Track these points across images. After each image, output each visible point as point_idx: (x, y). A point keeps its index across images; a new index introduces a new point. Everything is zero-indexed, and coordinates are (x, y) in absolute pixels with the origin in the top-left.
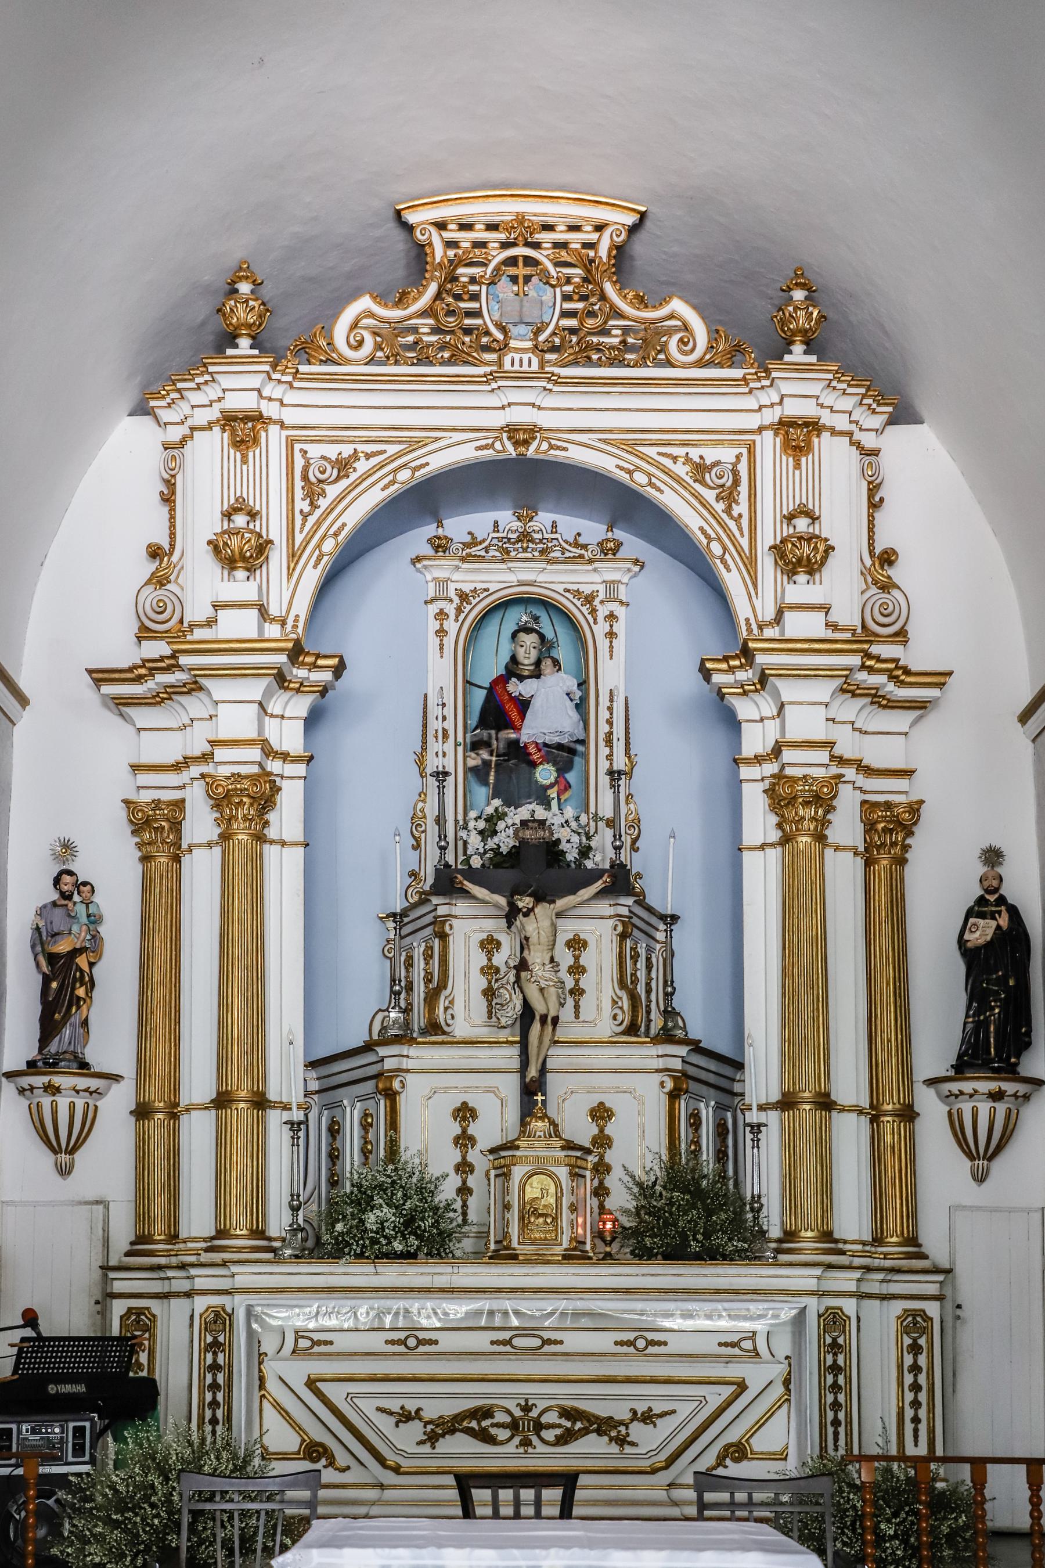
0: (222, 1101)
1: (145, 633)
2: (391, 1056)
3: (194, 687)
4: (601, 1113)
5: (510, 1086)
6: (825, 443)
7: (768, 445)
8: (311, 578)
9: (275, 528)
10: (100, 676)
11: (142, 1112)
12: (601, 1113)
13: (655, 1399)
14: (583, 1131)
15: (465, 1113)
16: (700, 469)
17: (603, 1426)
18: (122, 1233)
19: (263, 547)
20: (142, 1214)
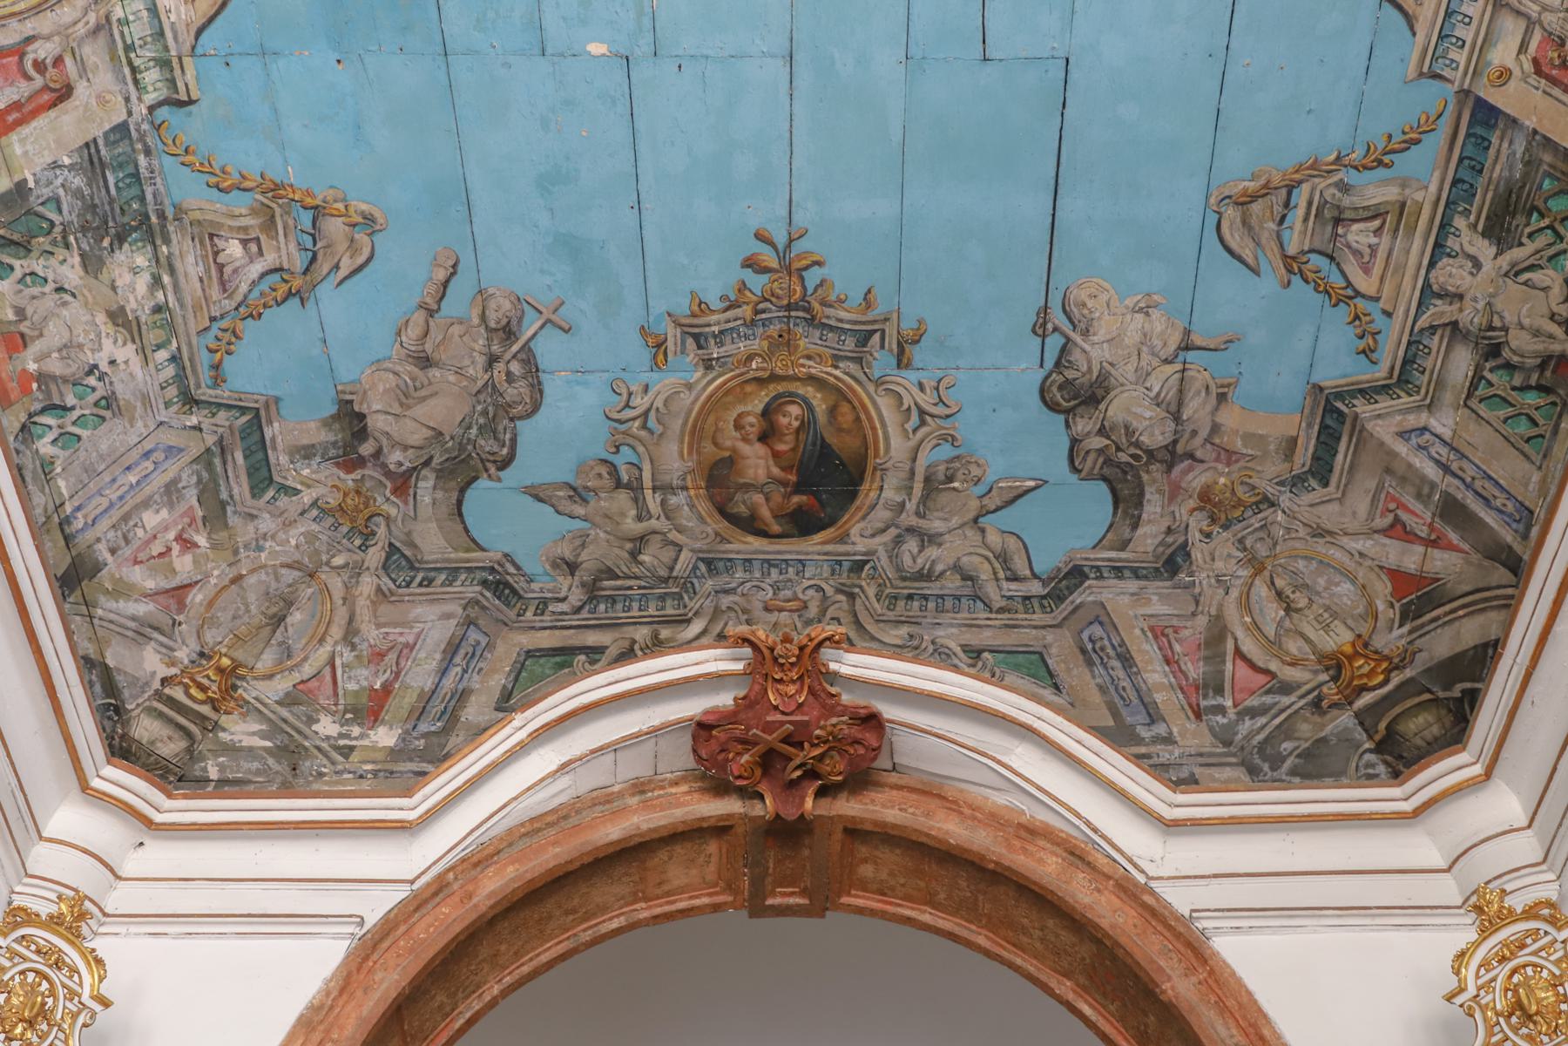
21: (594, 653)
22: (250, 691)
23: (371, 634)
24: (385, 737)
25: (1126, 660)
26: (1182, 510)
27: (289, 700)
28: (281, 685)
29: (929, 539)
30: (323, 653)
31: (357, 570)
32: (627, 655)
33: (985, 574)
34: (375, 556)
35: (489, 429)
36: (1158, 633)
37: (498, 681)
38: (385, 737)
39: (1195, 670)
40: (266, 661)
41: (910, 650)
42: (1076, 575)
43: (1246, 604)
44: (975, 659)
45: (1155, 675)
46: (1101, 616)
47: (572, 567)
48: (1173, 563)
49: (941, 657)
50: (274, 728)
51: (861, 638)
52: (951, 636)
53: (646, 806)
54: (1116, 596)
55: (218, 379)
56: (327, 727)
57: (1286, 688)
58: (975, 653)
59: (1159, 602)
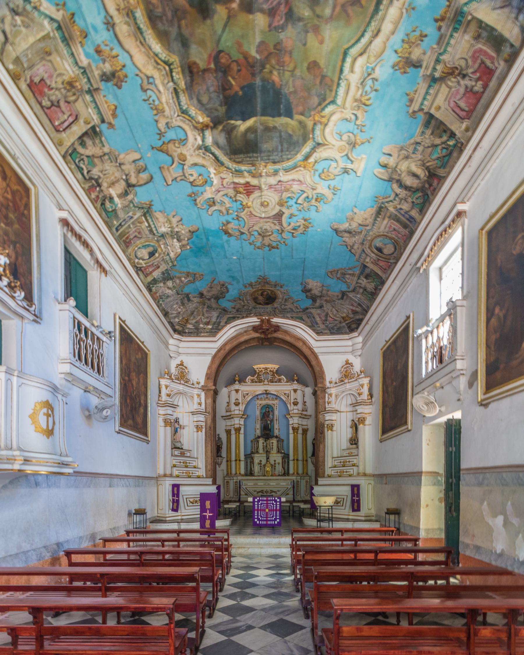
0: (236, 460)
1: (227, 411)
2: (253, 455)
3: (232, 418)
4: (275, 461)
5: (265, 458)
6: (298, 391)
7: (292, 391)
8: (244, 406)
9: (240, 401)
10: (222, 417)
11: (227, 461)
12: (275, 461)
13: (279, 489)
14: (273, 463)
15: (261, 461)
16: (285, 394)
17: (274, 492)
18: (225, 474)
19: (239, 403)
20: (227, 471)
21: (238, 317)
22: (190, 321)
23: (206, 315)
24: (210, 327)
25: (314, 318)
26: (322, 302)
27: (196, 322)
28: (194, 321)
29: (285, 305)
30: (199, 317)
31: (203, 308)
32: (243, 318)
33: (294, 309)
34: (206, 307)
35: (221, 294)
36: (318, 314)
37: (225, 320)
38: (210, 327)
39: (323, 318)
40: (192, 318)
41: (283, 317)
42: (307, 309)
43: (331, 311)
44: (292, 318)
45: (318, 319)
46: (311, 313)
47: (234, 308)
48: (321, 307)
49: (288, 318)
50: (194, 326)
51: (276, 316)
52: (289, 315)
53: (247, 335)
54: (313, 311)
55: (182, 291)
56: (201, 326)
57: (336, 320)
58: (292, 317)
59: (319, 311)
